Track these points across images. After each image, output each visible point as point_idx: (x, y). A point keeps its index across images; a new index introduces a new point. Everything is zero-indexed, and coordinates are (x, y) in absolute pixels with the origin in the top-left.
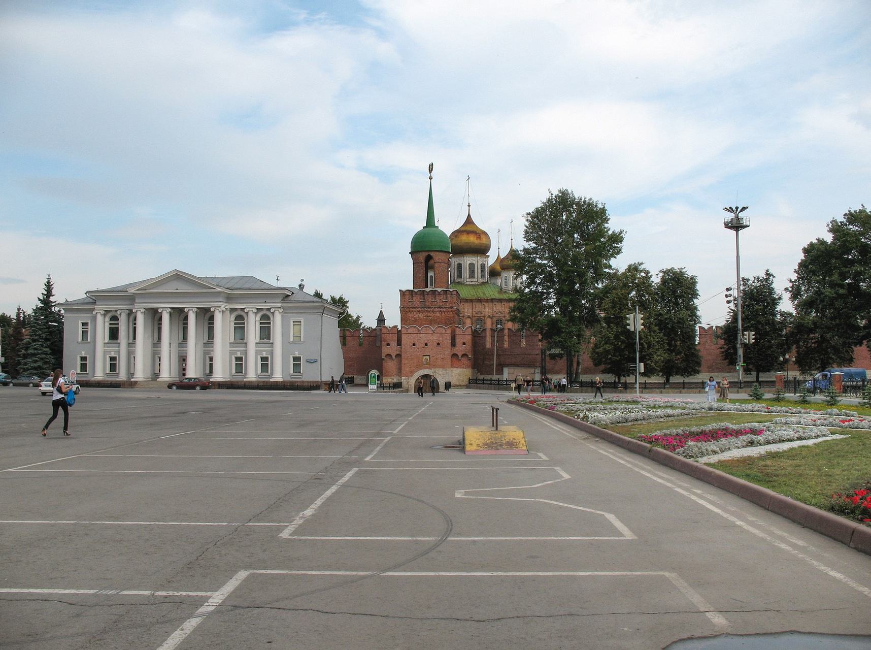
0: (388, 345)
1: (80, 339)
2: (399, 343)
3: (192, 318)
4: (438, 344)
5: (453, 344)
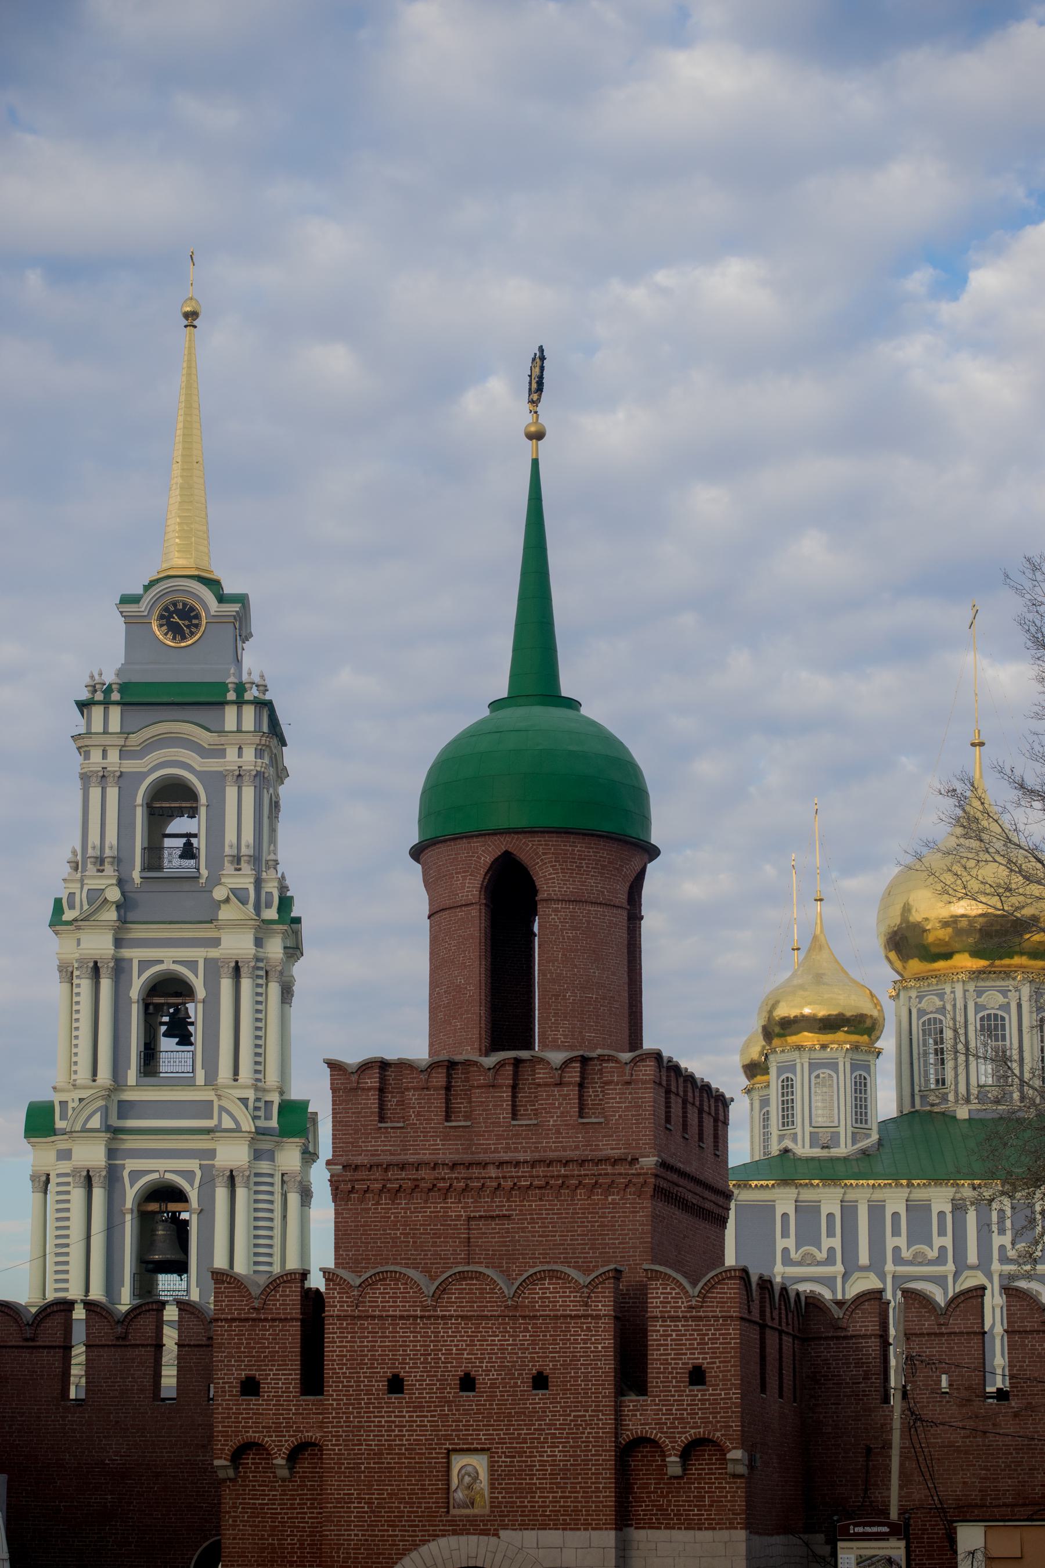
0: (250, 1387)
4: (540, 1381)
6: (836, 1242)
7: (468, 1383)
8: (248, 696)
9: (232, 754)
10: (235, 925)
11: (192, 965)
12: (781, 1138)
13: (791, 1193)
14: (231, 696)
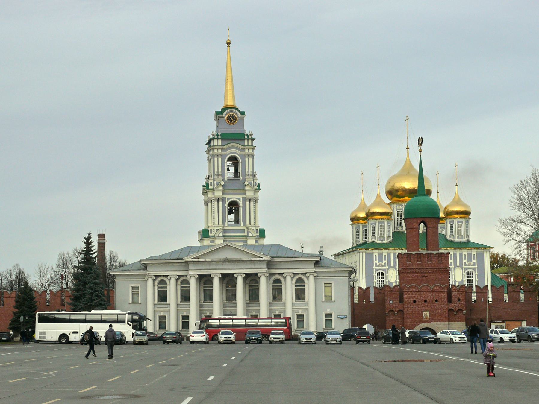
1: (131, 302)
2: (401, 300)
3: (240, 282)
5: (450, 300)
6: (386, 262)
7: (425, 301)
8: (250, 137)
9: (247, 151)
10: (249, 190)
11: (239, 199)
12: (372, 238)
13: (377, 251)
14: (246, 137)
